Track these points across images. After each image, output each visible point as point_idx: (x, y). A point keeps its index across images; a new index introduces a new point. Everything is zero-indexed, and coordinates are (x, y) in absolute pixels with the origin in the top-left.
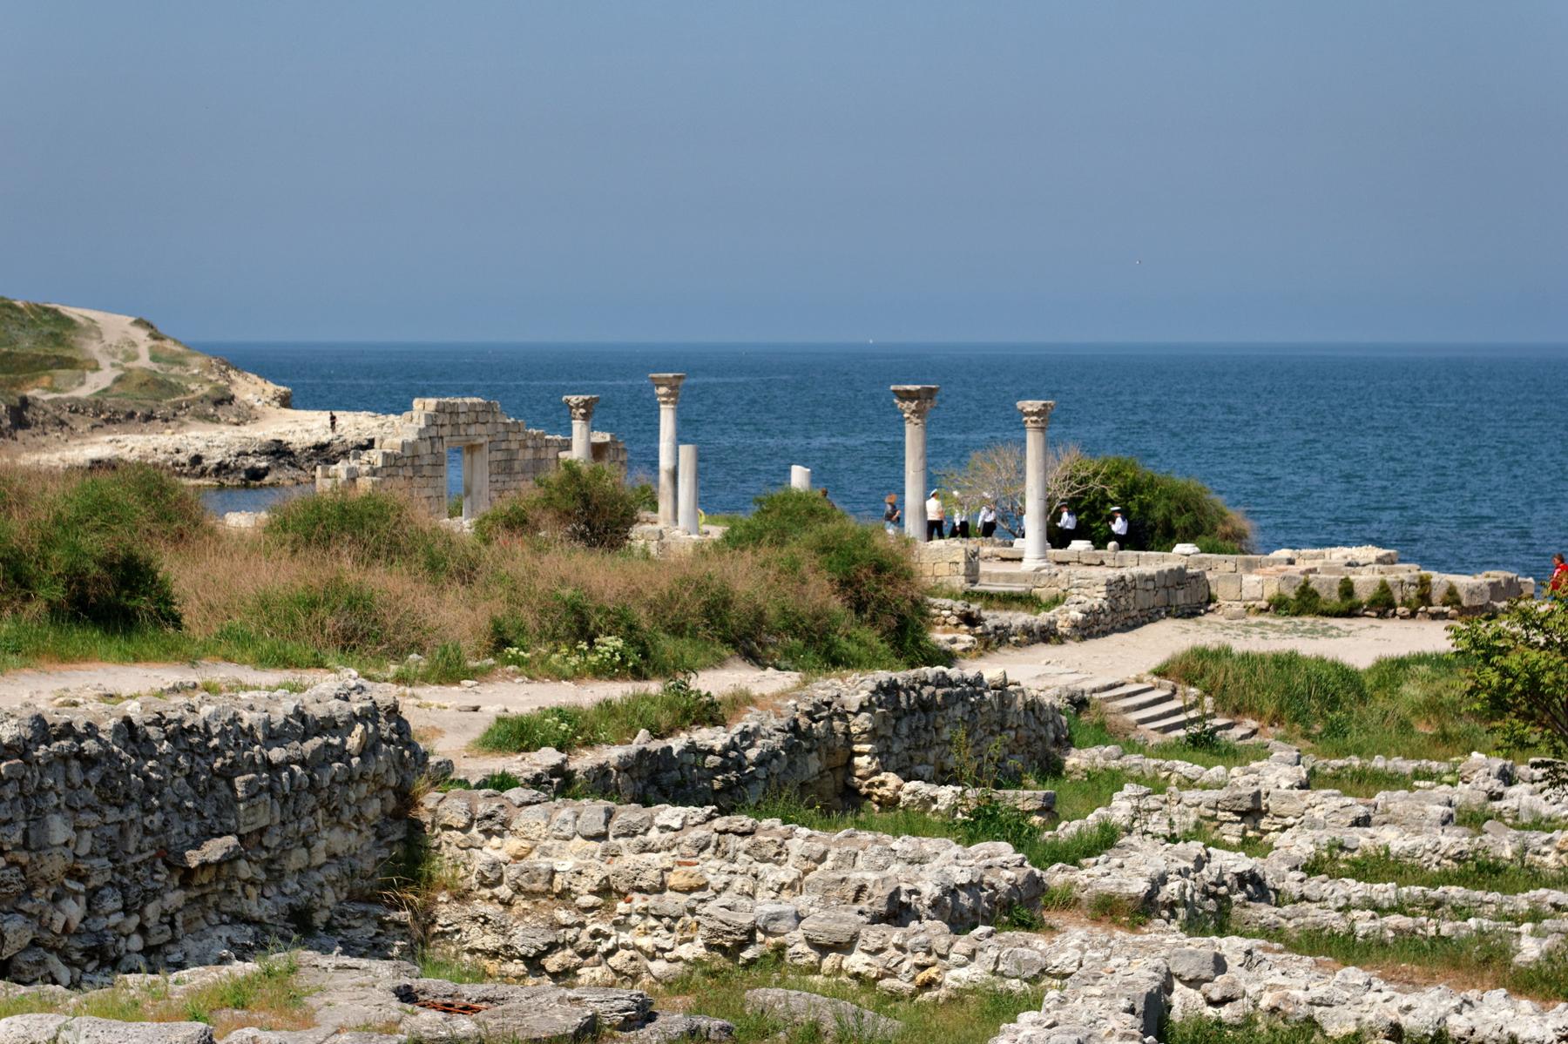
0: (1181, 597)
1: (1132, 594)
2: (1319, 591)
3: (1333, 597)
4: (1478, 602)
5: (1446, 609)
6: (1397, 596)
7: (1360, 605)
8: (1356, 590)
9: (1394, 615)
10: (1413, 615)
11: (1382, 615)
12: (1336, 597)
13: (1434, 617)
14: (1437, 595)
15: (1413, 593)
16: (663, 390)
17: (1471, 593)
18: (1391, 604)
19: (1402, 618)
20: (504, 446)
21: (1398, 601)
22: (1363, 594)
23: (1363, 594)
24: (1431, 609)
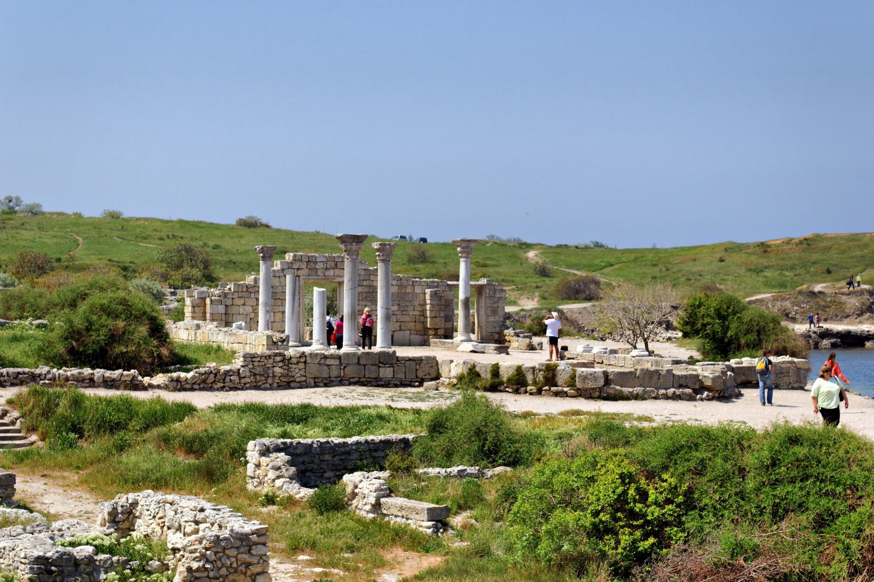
0: (386, 373)
1: (302, 366)
2: (481, 372)
3: (486, 376)
4: (590, 385)
5: (565, 389)
6: (530, 378)
7: (502, 383)
8: (501, 373)
9: (526, 392)
10: (539, 392)
11: (516, 392)
12: (489, 376)
13: (557, 394)
14: (562, 378)
15: (540, 377)
16: (459, 249)
17: (585, 378)
18: (525, 384)
19: (531, 394)
20: (365, 283)
21: (530, 382)
22: (505, 375)
23: (505, 375)
24: (552, 388)
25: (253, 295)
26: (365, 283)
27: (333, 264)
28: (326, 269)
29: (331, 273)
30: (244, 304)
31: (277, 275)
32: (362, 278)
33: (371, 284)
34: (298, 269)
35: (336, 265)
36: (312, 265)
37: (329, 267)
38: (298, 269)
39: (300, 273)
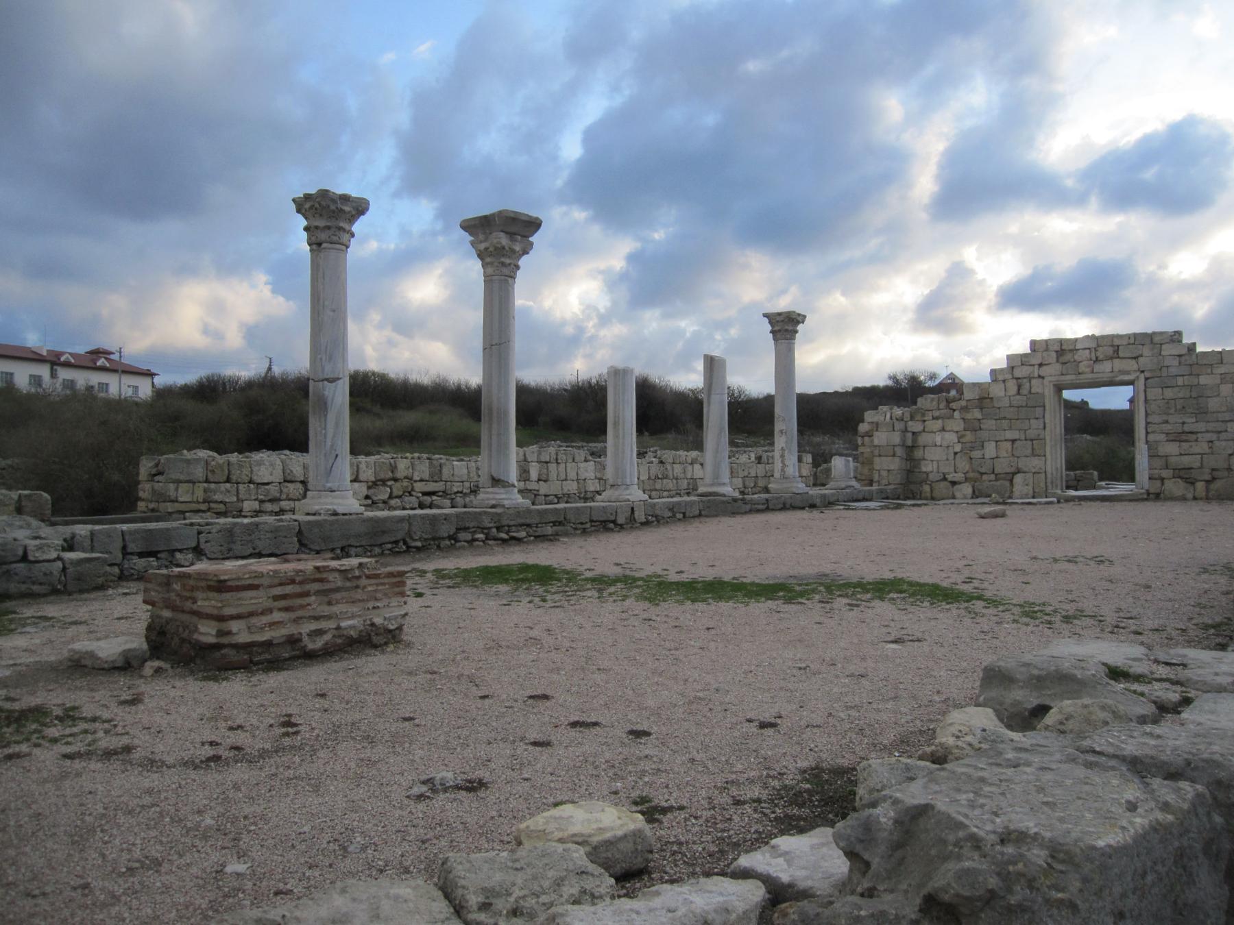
20: (1180, 381)
25: (956, 414)
26: (1180, 381)
27: (1110, 351)
28: (1097, 360)
29: (1106, 367)
30: (943, 430)
31: (1001, 378)
32: (1173, 371)
33: (1195, 381)
34: (1040, 365)
35: (1117, 351)
36: (1068, 357)
37: (1101, 357)
38: (1040, 365)
39: (1045, 371)
